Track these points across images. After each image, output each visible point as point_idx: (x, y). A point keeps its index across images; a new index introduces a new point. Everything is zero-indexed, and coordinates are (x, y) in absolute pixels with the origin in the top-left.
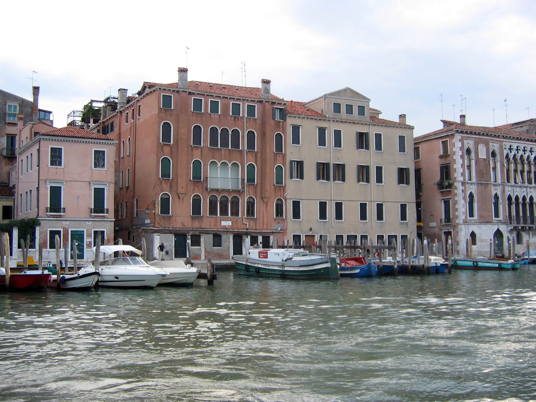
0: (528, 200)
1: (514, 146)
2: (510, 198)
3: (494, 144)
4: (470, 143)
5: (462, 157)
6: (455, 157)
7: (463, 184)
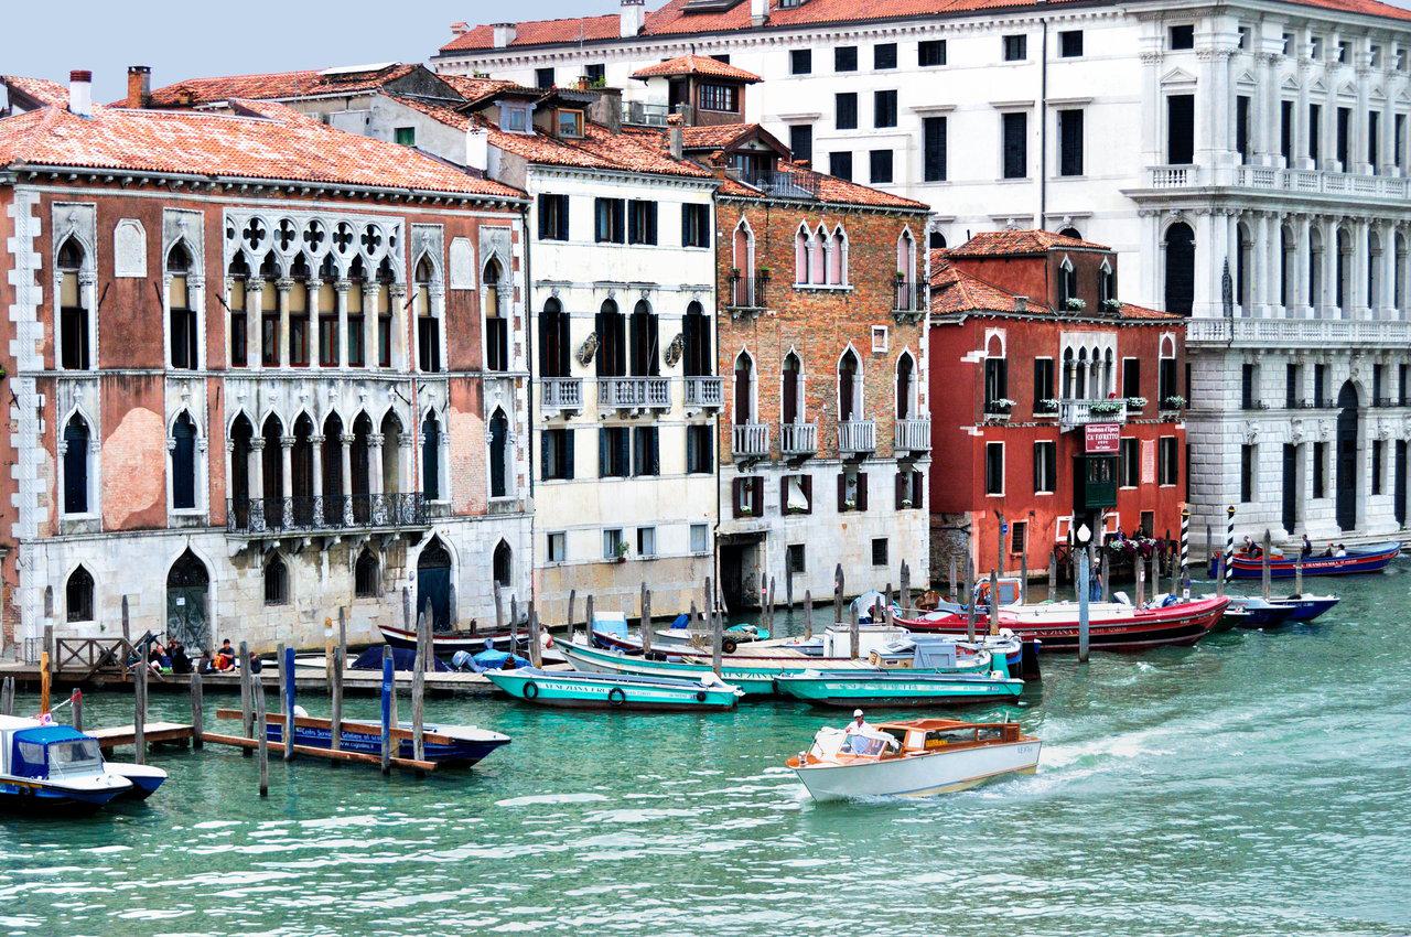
0: (318, 432)
1: (271, 222)
2: (241, 427)
3: (184, 218)
4: (78, 219)
5: (42, 277)
6: (13, 277)
7: (44, 382)
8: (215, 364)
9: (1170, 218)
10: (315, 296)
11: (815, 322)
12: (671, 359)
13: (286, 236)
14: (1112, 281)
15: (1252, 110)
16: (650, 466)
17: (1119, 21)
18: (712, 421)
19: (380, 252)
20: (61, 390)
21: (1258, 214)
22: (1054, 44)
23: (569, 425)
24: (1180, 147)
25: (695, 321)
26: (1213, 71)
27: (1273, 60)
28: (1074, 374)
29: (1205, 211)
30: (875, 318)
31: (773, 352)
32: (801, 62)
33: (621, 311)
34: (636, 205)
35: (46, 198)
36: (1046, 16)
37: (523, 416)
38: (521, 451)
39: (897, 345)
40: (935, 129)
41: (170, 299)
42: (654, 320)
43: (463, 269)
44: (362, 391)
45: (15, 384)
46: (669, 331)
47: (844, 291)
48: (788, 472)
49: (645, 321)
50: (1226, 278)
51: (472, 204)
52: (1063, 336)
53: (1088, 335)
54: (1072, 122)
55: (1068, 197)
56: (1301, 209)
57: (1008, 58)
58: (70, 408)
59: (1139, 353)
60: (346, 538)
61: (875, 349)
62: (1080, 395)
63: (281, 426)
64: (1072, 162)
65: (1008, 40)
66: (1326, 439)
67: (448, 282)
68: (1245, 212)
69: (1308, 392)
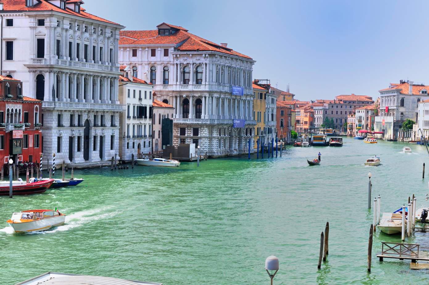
9: (38, 73)
14: (21, 90)
15: (61, 44)
17: (24, 17)
24: (40, 53)
26: (50, 32)
27: (67, 30)
28: (10, 116)
29: (47, 71)
52: (7, 105)
53: (14, 105)
56: (74, 72)
62: (12, 122)
66: (81, 135)
69: (76, 123)
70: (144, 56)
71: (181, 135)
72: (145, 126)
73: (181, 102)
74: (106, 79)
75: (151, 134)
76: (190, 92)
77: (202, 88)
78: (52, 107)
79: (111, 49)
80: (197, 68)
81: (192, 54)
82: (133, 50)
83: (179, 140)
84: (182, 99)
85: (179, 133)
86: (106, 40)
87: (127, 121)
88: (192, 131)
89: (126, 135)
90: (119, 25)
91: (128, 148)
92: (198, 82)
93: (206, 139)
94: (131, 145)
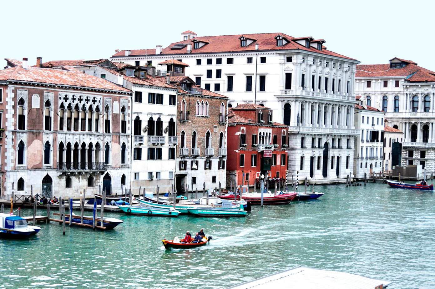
0: (80, 147)
1: (70, 96)
2: (61, 145)
3: (49, 94)
4: (23, 94)
5: (14, 107)
6: (7, 107)
7: (14, 133)
8: (56, 130)
9: (285, 102)
10: (80, 114)
11: (200, 124)
12: (166, 132)
13: (74, 99)
14: (271, 116)
15: (305, 77)
16: (160, 157)
17: (275, 55)
18: (175, 147)
19: (96, 104)
20: (18, 135)
21: (306, 102)
22: (259, 60)
23: (140, 147)
24: (288, 85)
25: (171, 123)
27: (310, 66)
28: (262, 138)
29: (294, 101)
30: (215, 124)
31: (190, 131)
32: (199, 62)
33: (154, 120)
34: (158, 95)
35: (16, 88)
36: (257, 53)
37: (130, 144)
38: (129, 153)
39: (220, 130)
40: (230, 79)
41: (45, 113)
42: (162, 122)
43: (116, 108)
44: (91, 137)
45: (7, 133)
46: (165, 125)
47: (207, 117)
48: (193, 160)
49: (160, 122)
50: (298, 117)
51: (119, 93)
52: (259, 129)
53: (265, 129)
54: (263, 79)
55: (261, 96)
56: (316, 101)
57: (248, 63)
58: (20, 139)
59: (277, 134)
60: (86, 173)
61: (214, 131)
62: (263, 143)
63: (71, 145)
64: (262, 88)
65: (248, 58)
67: (112, 112)
68: (303, 102)
69: (316, 144)
70: (377, 87)
71: (409, 157)
72: (377, 148)
73: (410, 128)
74: (343, 107)
75: (382, 156)
76: (418, 119)
77: (431, 115)
78: (297, 131)
79: (348, 82)
80: (425, 98)
81: (421, 86)
82: (367, 82)
83: (408, 162)
84: (411, 125)
85: (408, 155)
86: (344, 74)
87: (361, 144)
88: (419, 154)
89: (360, 156)
90: (356, 60)
91: (361, 167)
92: (426, 109)
93: (433, 161)
94: (364, 165)
